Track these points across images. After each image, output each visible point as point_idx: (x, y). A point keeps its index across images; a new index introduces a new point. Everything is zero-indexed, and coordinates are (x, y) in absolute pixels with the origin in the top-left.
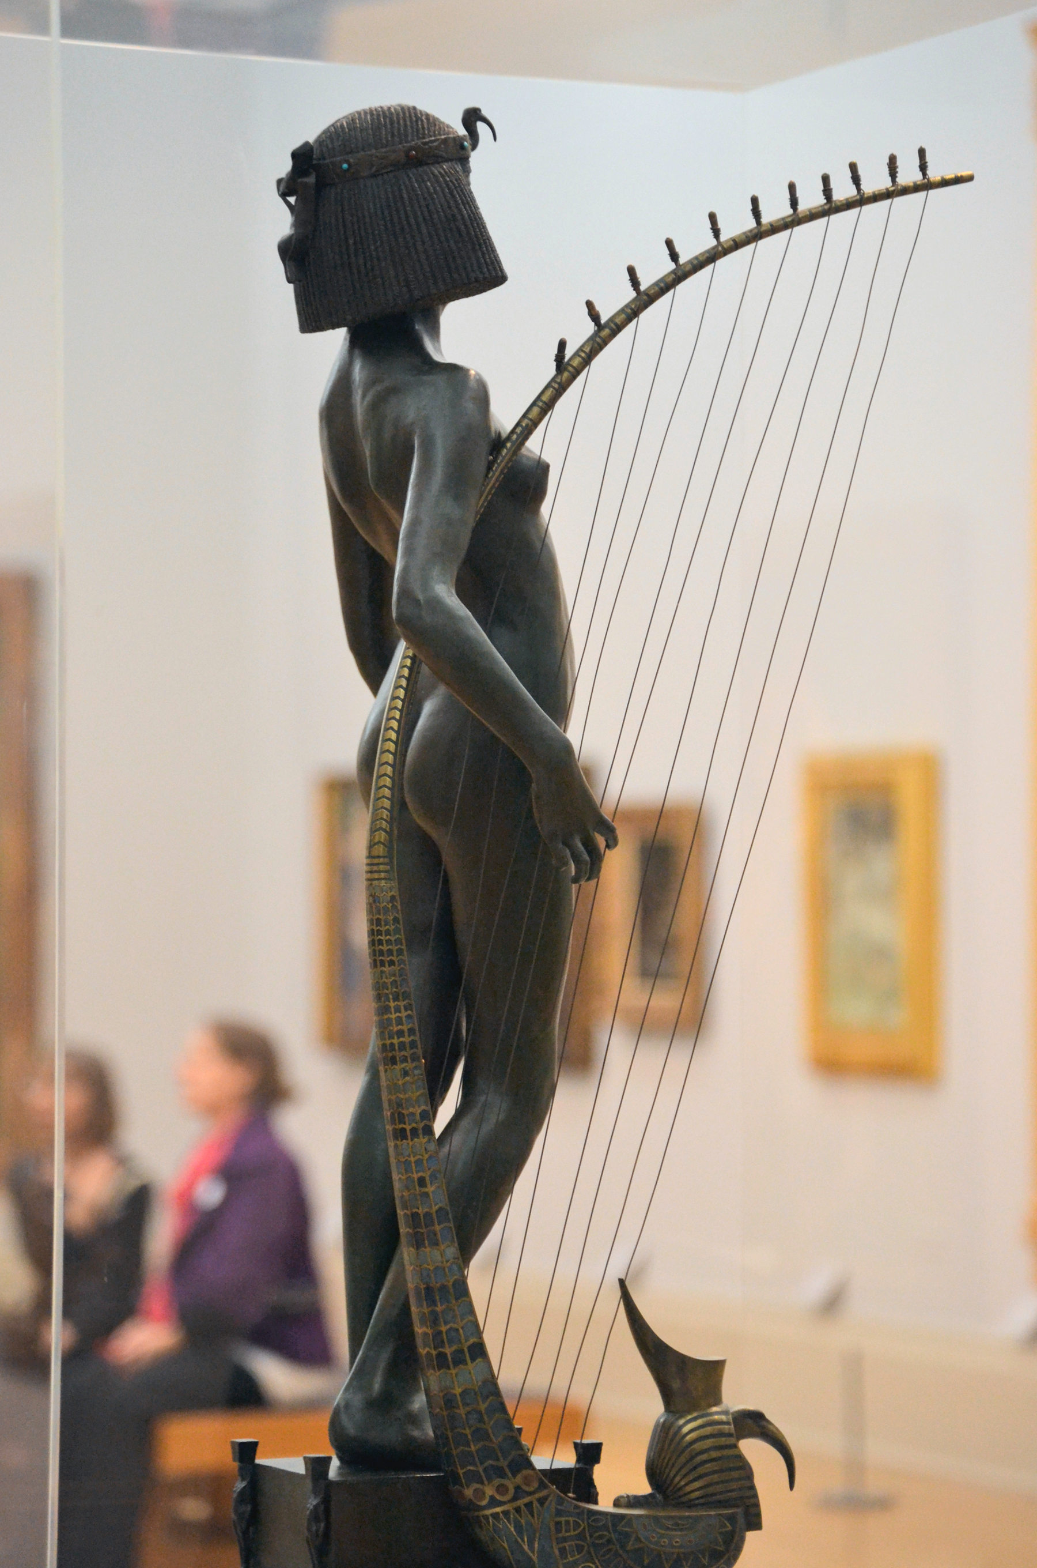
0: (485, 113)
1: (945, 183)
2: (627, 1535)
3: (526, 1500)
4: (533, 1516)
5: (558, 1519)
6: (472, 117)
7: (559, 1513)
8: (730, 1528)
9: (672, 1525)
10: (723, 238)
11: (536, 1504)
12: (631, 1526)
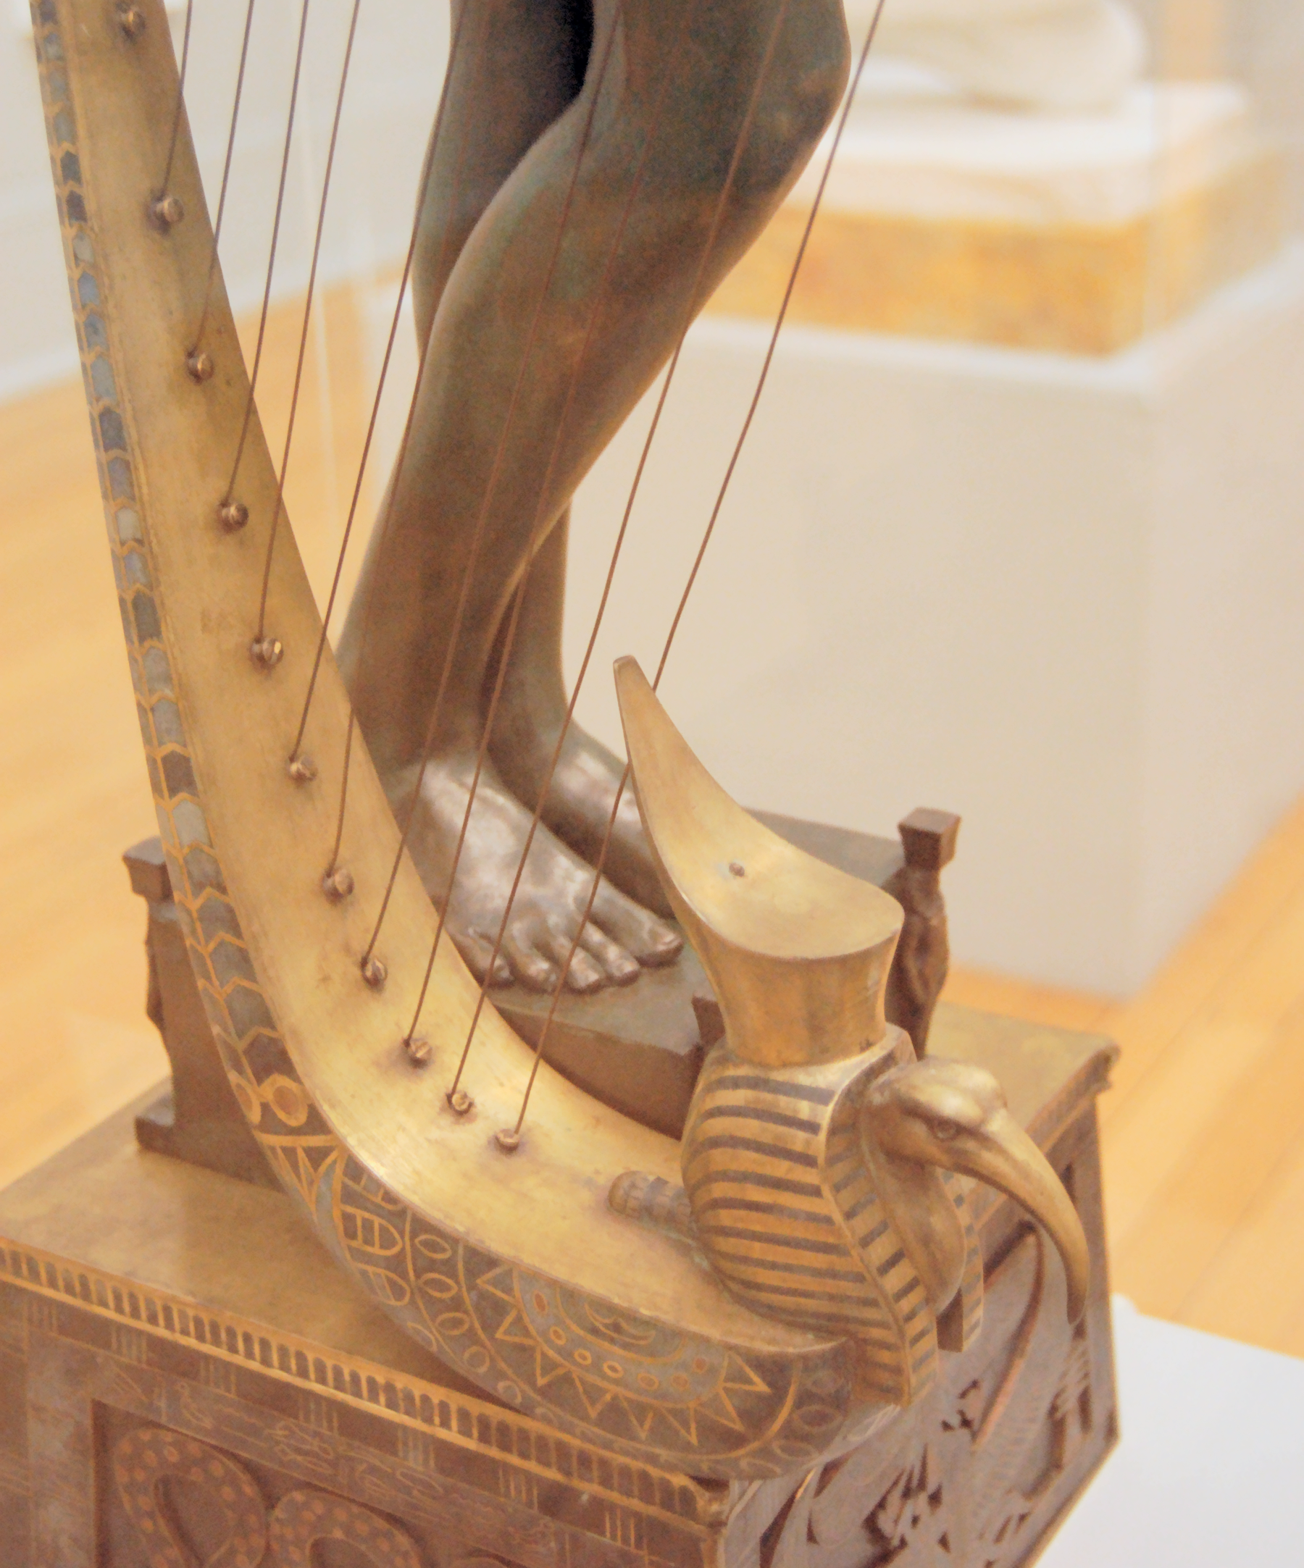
2: (500, 1309)
5: (350, 1209)
7: (349, 1196)
8: (761, 1386)
9: (606, 1326)
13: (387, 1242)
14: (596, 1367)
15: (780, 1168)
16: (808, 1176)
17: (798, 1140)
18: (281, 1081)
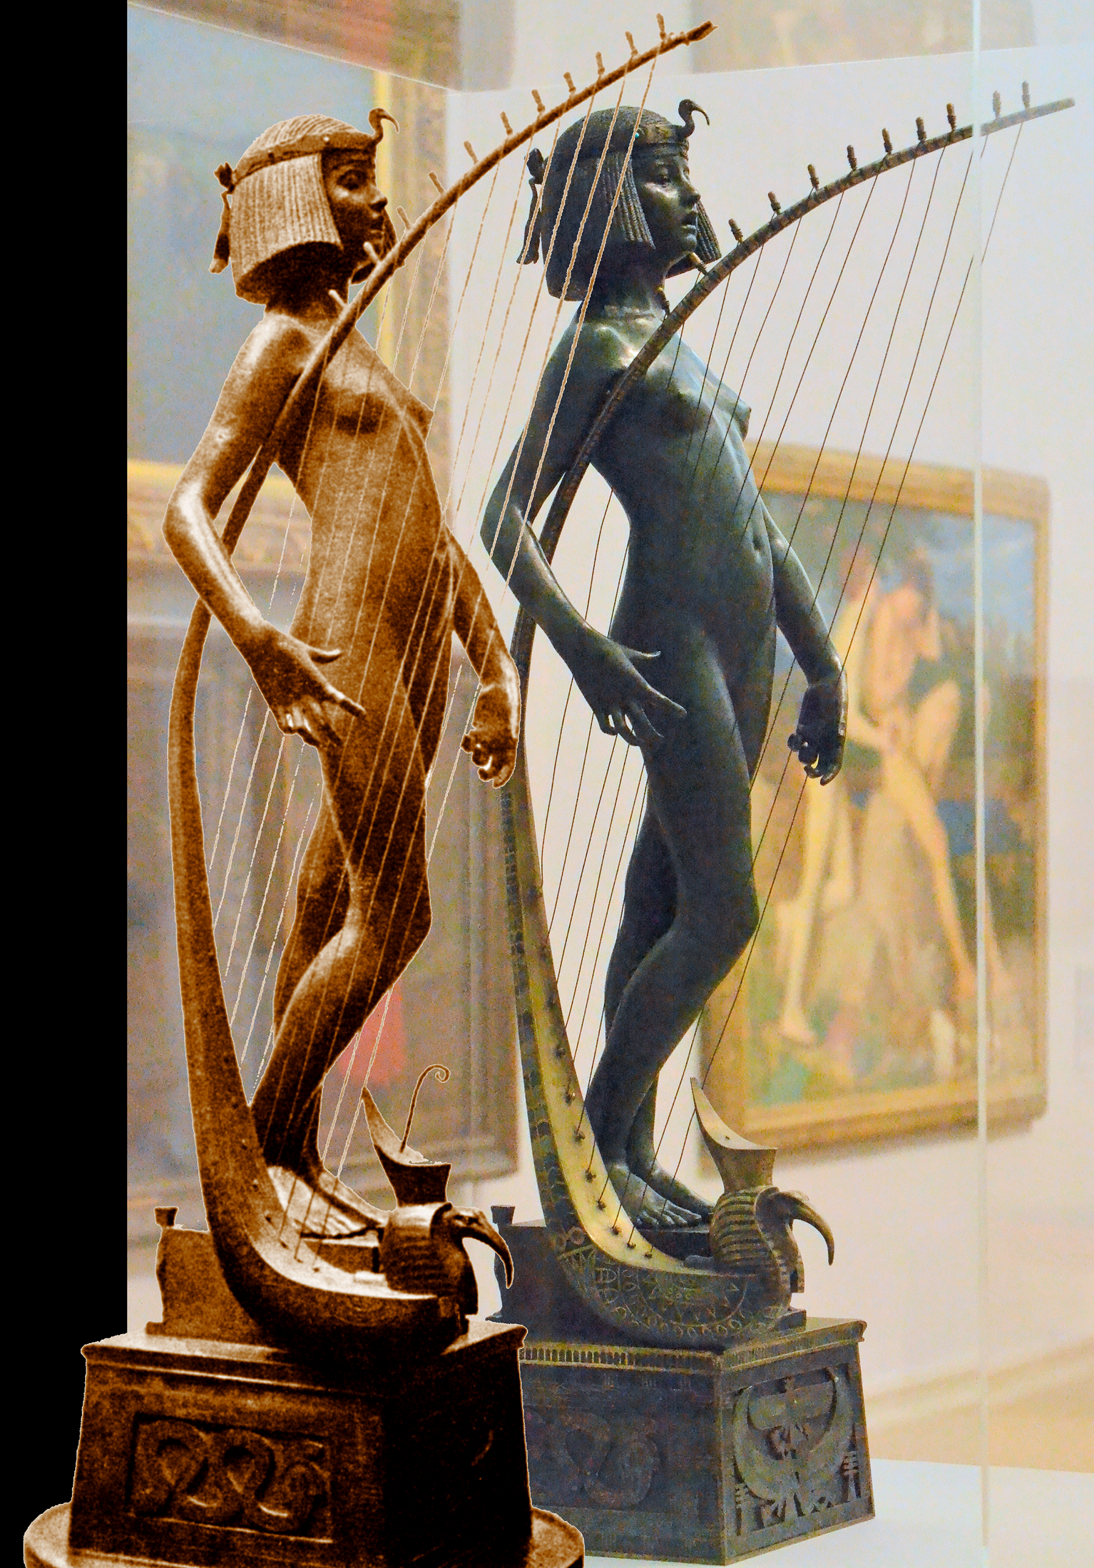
0: (697, 102)
1: (1042, 111)
3: (575, 1251)
4: (579, 1263)
5: (598, 1269)
6: (687, 108)
7: (599, 1264)
10: (821, 186)
11: (582, 1257)
12: (653, 1279)
13: (611, 1276)
14: (684, 1298)
15: (745, 1218)
16: (753, 1218)
17: (747, 1207)
18: (574, 1229)
